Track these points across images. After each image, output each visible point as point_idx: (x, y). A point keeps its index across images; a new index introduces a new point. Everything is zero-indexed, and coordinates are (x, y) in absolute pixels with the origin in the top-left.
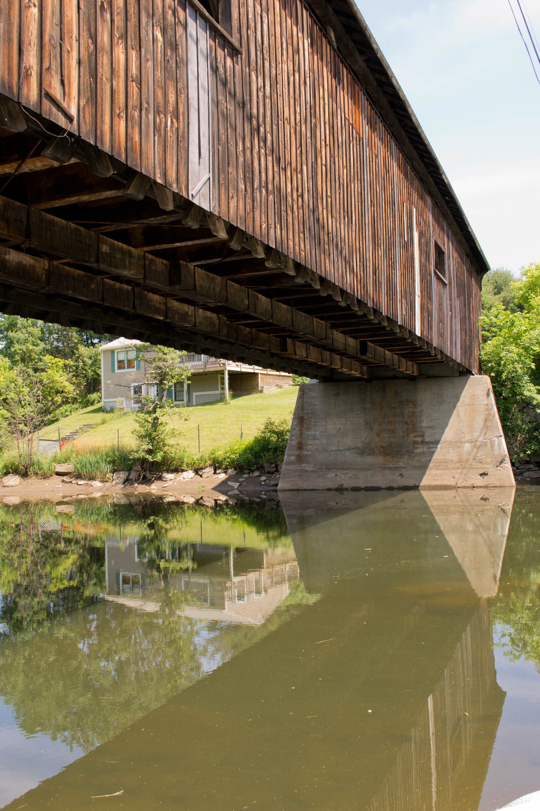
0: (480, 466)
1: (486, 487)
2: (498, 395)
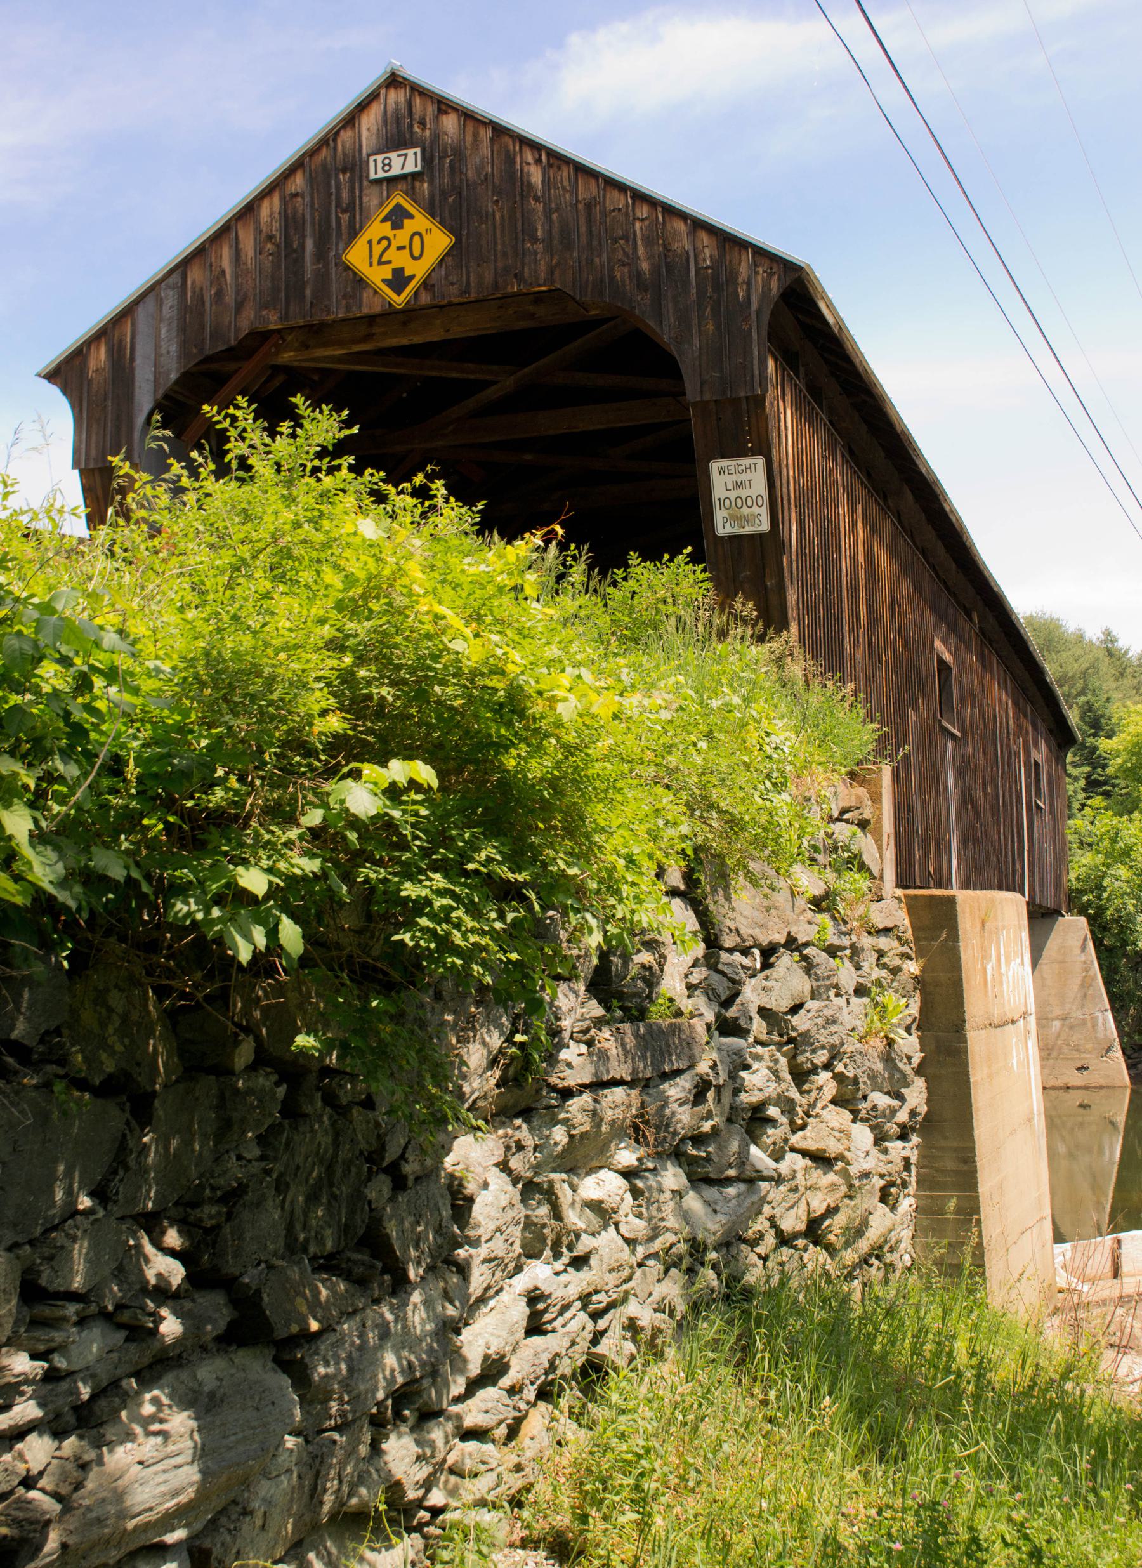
0: (1076, 1055)
1: (1086, 1088)
2: (1098, 944)
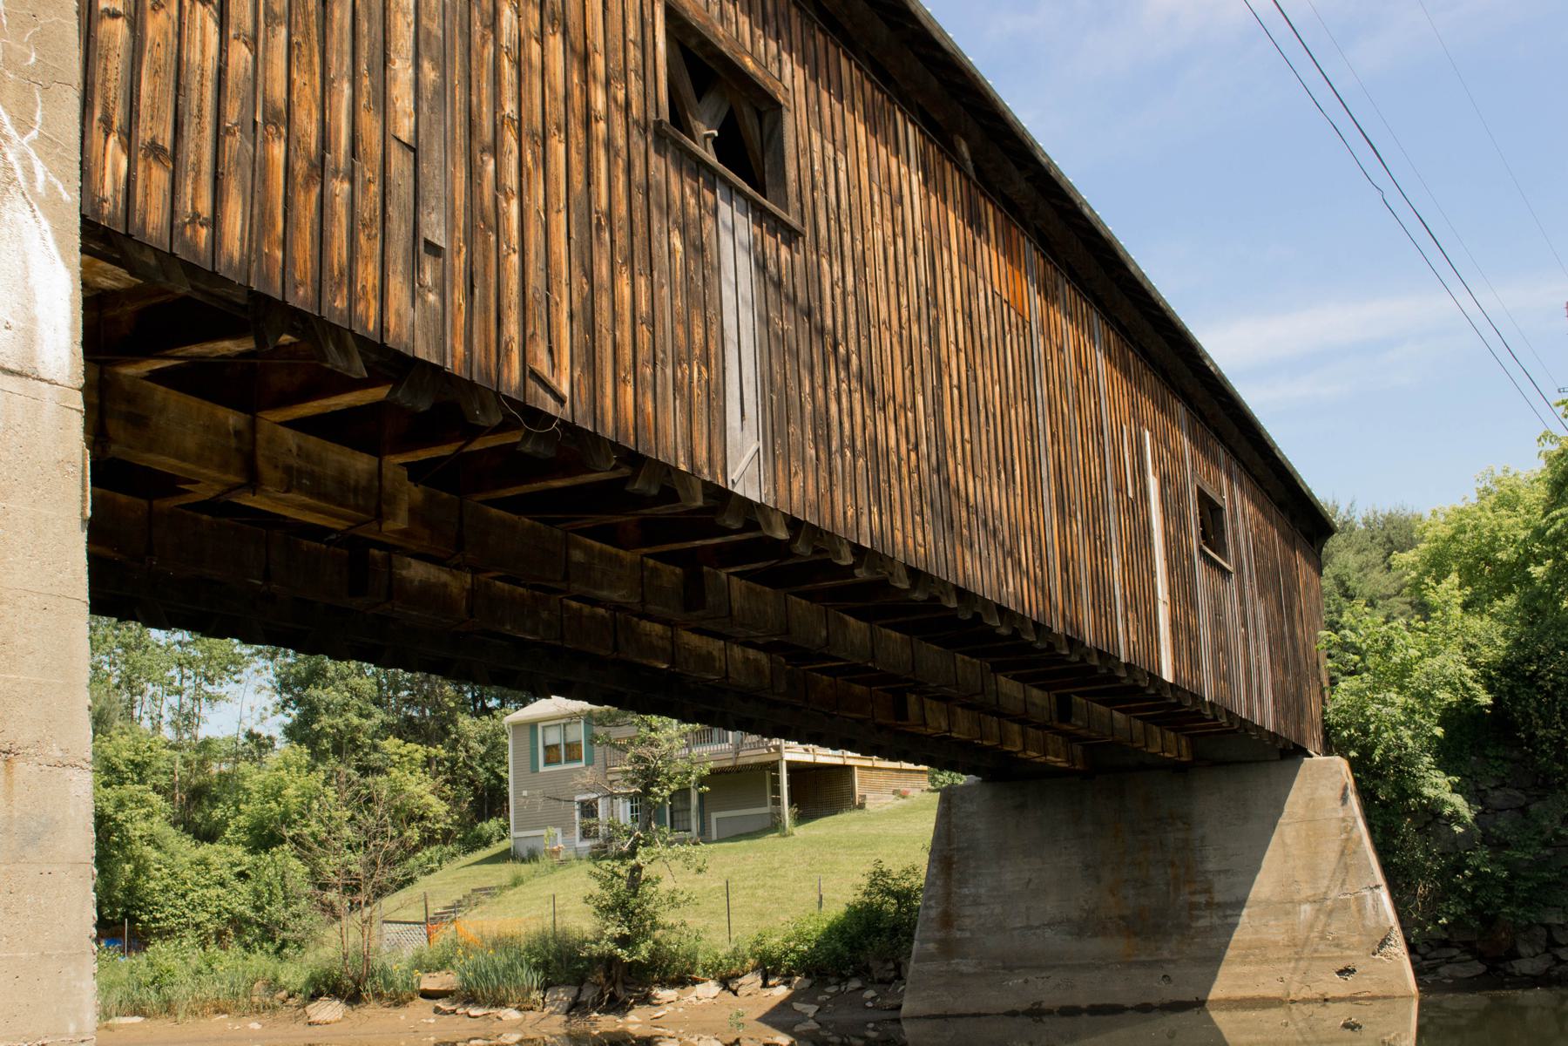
0: (1337, 952)
1: (1353, 999)
2: (1367, 797)
